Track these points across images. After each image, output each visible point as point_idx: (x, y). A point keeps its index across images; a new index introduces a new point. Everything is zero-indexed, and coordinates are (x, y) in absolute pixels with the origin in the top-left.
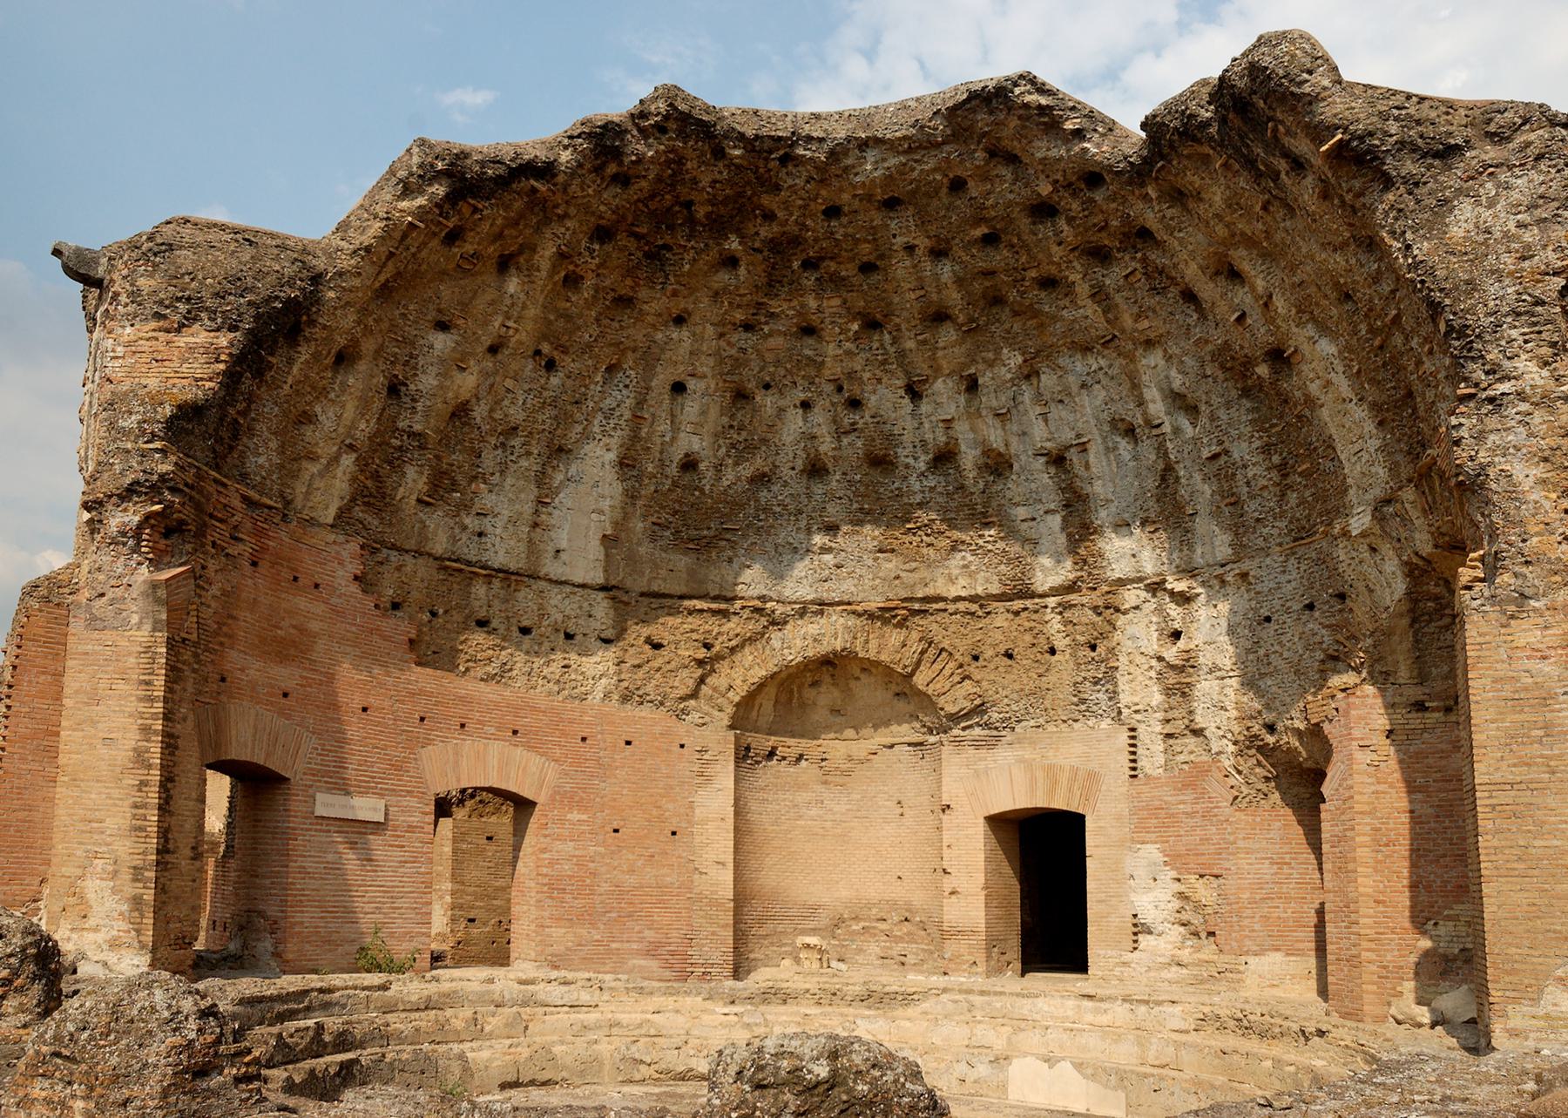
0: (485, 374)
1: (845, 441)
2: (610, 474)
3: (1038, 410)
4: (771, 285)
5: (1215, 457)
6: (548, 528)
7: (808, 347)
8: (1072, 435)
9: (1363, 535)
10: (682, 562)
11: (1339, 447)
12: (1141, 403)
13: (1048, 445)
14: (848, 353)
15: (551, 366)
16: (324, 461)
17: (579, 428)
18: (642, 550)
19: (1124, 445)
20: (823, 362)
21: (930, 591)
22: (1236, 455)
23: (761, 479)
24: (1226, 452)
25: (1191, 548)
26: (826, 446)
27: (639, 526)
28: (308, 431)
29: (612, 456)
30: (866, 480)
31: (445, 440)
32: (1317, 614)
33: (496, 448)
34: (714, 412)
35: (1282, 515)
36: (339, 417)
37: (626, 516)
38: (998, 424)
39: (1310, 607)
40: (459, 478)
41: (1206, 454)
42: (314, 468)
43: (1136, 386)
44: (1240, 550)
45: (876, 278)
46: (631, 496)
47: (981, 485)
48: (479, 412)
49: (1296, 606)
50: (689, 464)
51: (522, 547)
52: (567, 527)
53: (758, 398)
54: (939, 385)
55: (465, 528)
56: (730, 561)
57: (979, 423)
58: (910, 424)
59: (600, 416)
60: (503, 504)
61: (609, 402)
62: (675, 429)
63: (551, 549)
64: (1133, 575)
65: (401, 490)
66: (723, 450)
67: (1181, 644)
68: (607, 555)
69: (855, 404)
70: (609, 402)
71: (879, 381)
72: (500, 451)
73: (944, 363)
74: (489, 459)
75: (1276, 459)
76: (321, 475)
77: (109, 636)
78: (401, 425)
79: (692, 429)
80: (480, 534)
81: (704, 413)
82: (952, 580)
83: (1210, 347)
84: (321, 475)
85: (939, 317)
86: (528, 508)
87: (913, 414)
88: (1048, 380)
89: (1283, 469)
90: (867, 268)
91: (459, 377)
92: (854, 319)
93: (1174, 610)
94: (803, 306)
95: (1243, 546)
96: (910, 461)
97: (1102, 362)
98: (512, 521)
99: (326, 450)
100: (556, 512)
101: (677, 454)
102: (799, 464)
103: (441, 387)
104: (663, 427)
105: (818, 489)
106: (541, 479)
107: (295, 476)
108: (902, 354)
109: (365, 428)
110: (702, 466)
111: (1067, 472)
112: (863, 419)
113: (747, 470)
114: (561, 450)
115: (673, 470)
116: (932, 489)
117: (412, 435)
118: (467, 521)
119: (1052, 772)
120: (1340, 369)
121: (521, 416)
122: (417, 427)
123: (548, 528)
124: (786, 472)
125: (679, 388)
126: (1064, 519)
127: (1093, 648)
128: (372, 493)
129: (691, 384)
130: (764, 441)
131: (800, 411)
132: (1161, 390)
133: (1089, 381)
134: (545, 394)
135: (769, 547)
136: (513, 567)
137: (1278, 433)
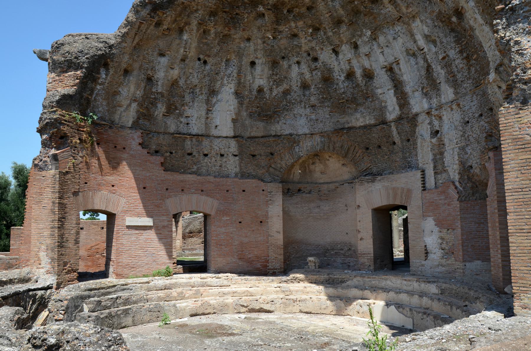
1: (314, 73)
2: (232, 97)
3: (380, 51)
4: (278, 22)
5: (444, 58)
8: (393, 58)
9: (494, 81)
10: (261, 125)
11: (484, 45)
12: (415, 42)
13: (386, 64)
14: (309, 41)
16: (125, 106)
17: (219, 82)
18: (247, 122)
19: (412, 61)
20: (301, 46)
21: (350, 125)
22: (451, 56)
24: (448, 56)
25: (440, 96)
28: (118, 97)
29: (233, 90)
30: (324, 87)
32: (483, 117)
33: (190, 93)
34: (266, 70)
35: (469, 79)
36: (129, 91)
38: (366, 57)
39: (481, 115)
40: (178, 105)
41: (440, 57)
42: (122, 109)
43: (412, 35)
44: (456, 93)
46: (241, 104)
47: (364, 83)
48: (181, 82)
49: (477, 115)
50: (260, 90)
51: (203, 126)
52: (219, 117)
53: (281, 63)
54: (343, 47)
55: (181, 122)
56: (278, 122)
57: (360, 59)
58: (336, 63)
59: (226, 77)
61: (229, 72)
62: (254, 78)
63: (214, 125)
64: (421, 110)
65: (156, 112)
66: (272, 83)
67: (439, 135)
68: (234, 125)
69: (315, 59)
70: (229, 72)
71: (322, 49)
72: (191, 94)
73: (344, 39)
74: (188, 98)
75: (465, 55)
76: (125, 111)
77: (44, 173)
78: (154, 90)
79: (260, 78)
80: (188, 124)
81: (262, 71)
82: (357, 120)
83: (435, 14)
84: (125, 111)
85: (338, 22)
86: (204, 113)
87: (337, 59)
88: (382, 39)
89: (468, 58)
91: (172, 72)
92: (309, 28)
93: (436, 123)
94: (290, 26)
95: (458, 93)
96: (338, 77)
97: (399, 28)
98: (199, 118)
99: (125, 103)
100: (214, 113)
101: (256, 86)
102: (299, 84)
103: (166, 76)
104: (249, 77)
105: (307, 93)
106: (208, 102)
107: (114, 113)
108: (328, 38)
109: (139, 94)
110: (265, 90)
111: (394, 73)
112: (319, 64)
113: (281, 89)
115: (255, 93)
116: (347, 87)
118: (182, 120)
119: (394, 189)
120: (477, 11)
121: (197, 81)
122: (159, 91)
124: (295, 88)
125: (253, 64)
126: (395, 91)
127: (408, 140)
128: (145, 115)
129: (257, 61)
130: (285, 78)
131: (297, 65)
132: (421, 35)
133: (396, 36)
134: (205, 72)
135: (292, 115)
136: (200, 133)
137: (465, 44)
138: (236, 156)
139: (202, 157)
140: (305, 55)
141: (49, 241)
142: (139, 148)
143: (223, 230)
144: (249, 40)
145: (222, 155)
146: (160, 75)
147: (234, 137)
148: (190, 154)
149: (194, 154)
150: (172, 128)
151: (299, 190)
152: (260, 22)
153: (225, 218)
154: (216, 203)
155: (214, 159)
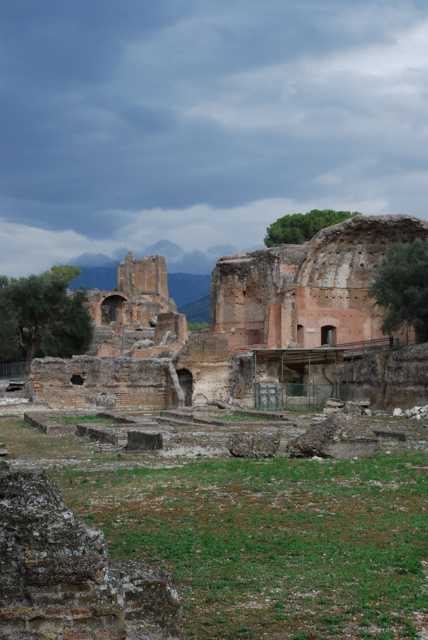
0: (328, 257)
6: (337, 279)
7: (383, 246)
10: (361, 282)
31: (321, 268)
46: (351, 272)
48: (327, 263)
50: (362, 265)
60: (330, 276)
68: (347, 282)
74: (328, 270)
77: (287, 310)
86: (334, 277)
90: (392, 235)
98: (331, 279)
101: (360, 264)
102: (382, 264)
114: (340, 265)
115: (359, 266)
117: (316, 269)
122: (317, 268)
123: (337, 279)
128: (311, 279)
129: (362, 252)
138: (347, 298)
139: (332, 298)
142: (309, 296)
143: (342, 335)
145: (341, 298)
147: (347, 288)
148: (326, 297)
149: (329, 297)
150: (320, 285)
153: (343, 329)
154: (339, 322)
155: (337, 300)
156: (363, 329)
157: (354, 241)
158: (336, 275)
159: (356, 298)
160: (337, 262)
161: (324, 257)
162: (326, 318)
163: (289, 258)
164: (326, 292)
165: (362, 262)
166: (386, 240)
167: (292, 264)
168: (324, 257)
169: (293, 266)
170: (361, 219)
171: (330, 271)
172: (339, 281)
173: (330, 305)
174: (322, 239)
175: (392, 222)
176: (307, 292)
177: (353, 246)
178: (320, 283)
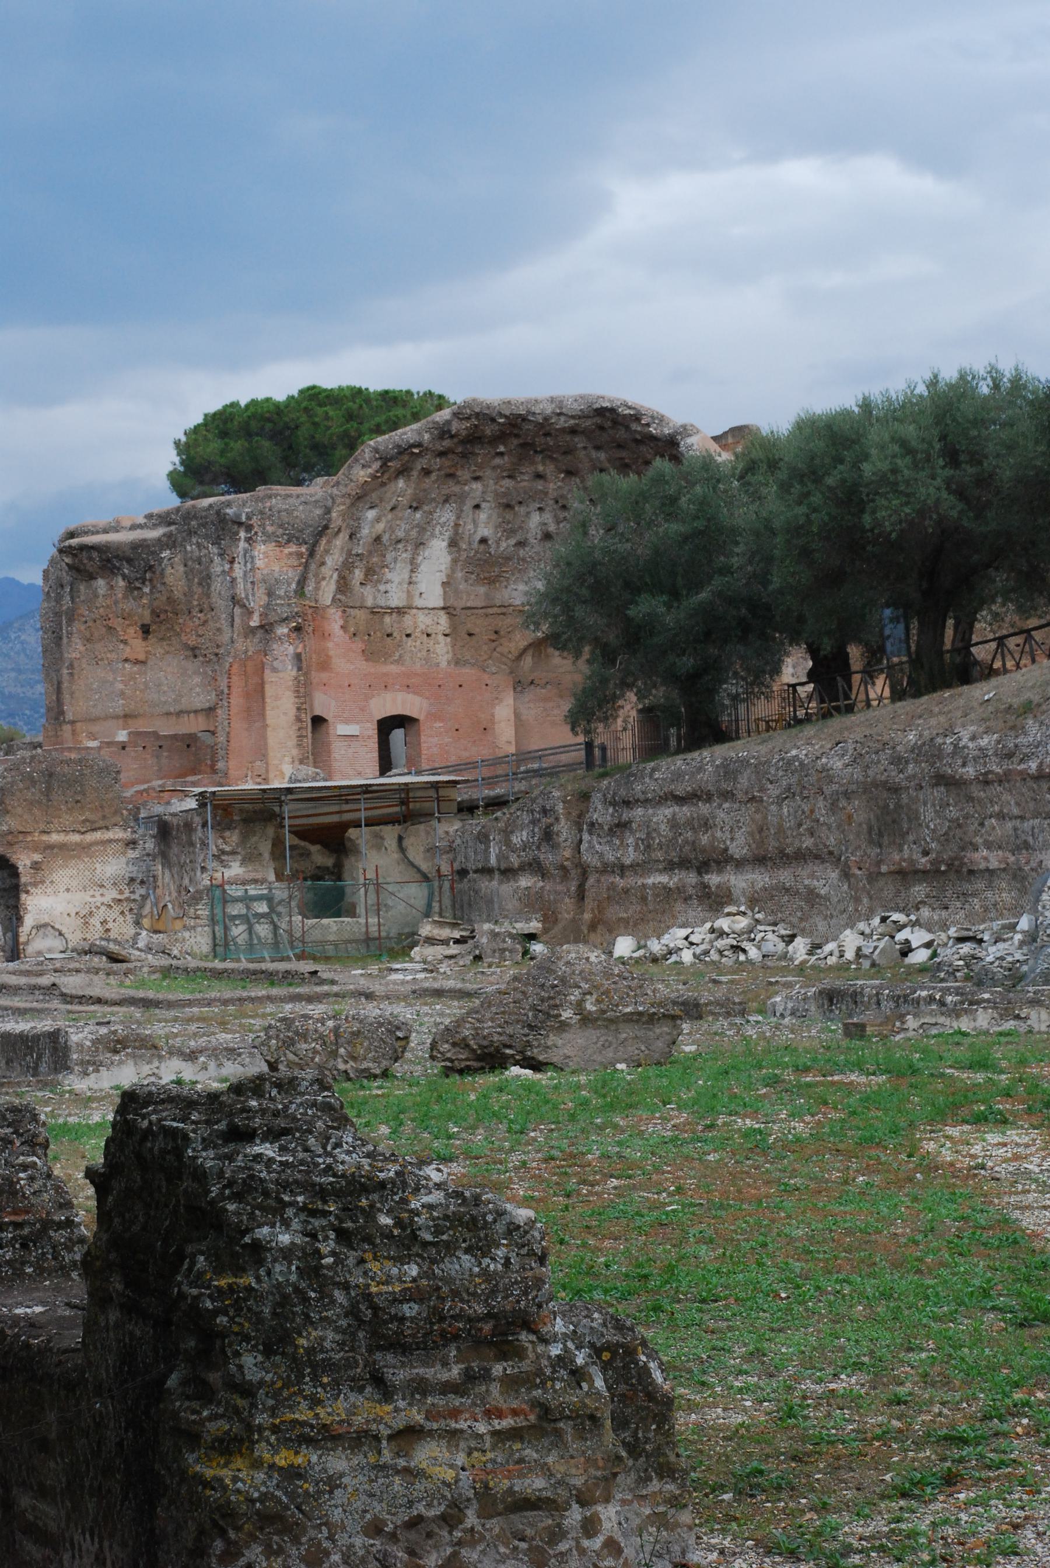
7: (540, 485)
10: (482, 590)
15: (416, 509)
23: (521, 544)
26: (552, 528)
27: (459, 575)
34: (495, 516)
37: (453, 570)
45: (569, 457)
46: (455, 561)
48: (385, 538)
50: (484, 541)
51: (405, 595)
68: (445, 592)
74: (389, 557)
77: (281, 675)
79: (484, 524)
81: (489, 517)
86: (406, 576)
101: (478, 538)
113: (512, 542)
115: (475, 545)
128: (343, 586)
130: (521, 528)
140: (551, 502)
141: (295, 752)
142: (341, 632)
144: (477, 479)
145: (428, 635)
146: (365, 531)
147: (443, 608)
150: (369, 603)
151: (532, 683)
152: (498, 461)
153: (438, 724)
156: (493, 723)
157: (459, 473)
158: (412, 571)
159: (470, 635)
160: (414, 533)
161: (378, 520)
162: (388, 696)
163: (281, 526)
164: (387, 619)
165: (484, 531)
166: (549, 469)
167: (289, 541)
168: (378, 520)
169: (293, 548)
170: (477, 410)
171: (395, 560)
172: (422, 587)
173: (400, 656)
174: (370, 471)
175: (562, 419)
176: (334, 621)
177: (456, 489)
178: (369, 596)
